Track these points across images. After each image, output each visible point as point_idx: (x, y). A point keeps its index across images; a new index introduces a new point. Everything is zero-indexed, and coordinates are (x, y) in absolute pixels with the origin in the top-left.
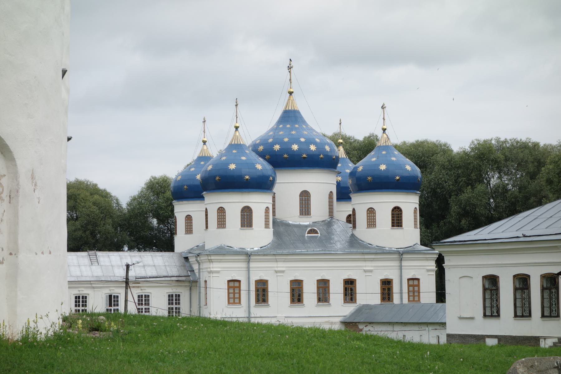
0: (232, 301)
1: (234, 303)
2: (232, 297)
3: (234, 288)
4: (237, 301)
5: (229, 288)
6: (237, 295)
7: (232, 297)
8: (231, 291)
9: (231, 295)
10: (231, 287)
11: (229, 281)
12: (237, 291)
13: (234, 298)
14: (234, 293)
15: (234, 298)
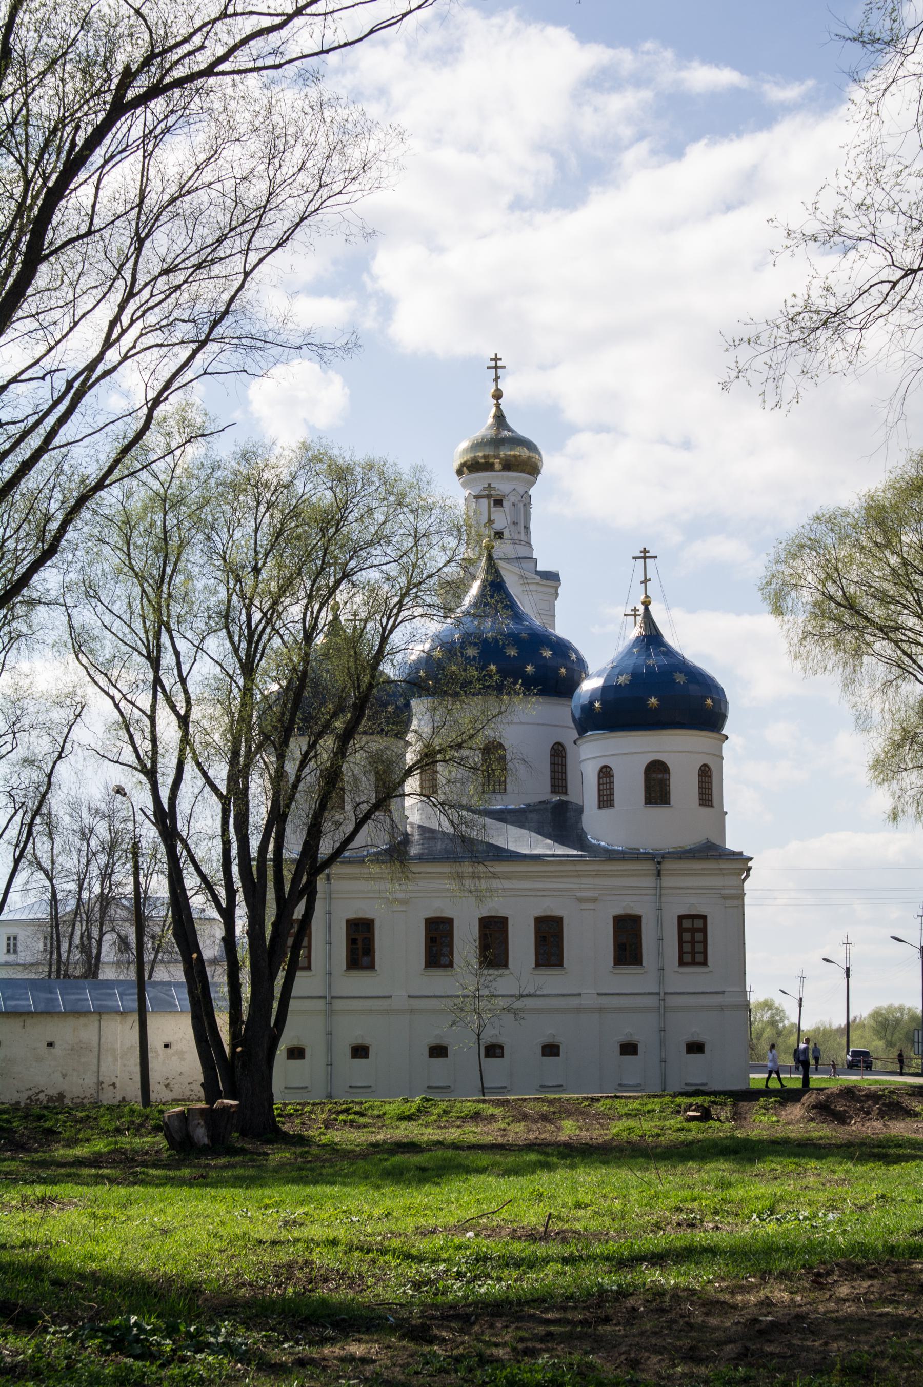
0: (687, 958)
1: (694, 963)
2: (689, 950)
3: (693, 931)
4: (699, 958)
5: (681, 930)
6: (699, 947)
7: (689, 950)
8: (687, 936)
9: (687, 948)
10: (687, 930)
11: (681, 918)
12: (699, 936)
13: (693, 953)
14: (693, 942)
15: (693, 953)
